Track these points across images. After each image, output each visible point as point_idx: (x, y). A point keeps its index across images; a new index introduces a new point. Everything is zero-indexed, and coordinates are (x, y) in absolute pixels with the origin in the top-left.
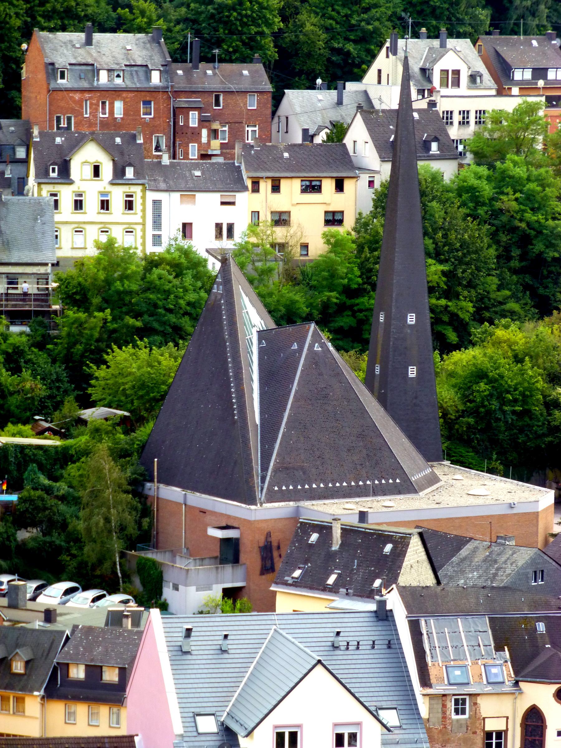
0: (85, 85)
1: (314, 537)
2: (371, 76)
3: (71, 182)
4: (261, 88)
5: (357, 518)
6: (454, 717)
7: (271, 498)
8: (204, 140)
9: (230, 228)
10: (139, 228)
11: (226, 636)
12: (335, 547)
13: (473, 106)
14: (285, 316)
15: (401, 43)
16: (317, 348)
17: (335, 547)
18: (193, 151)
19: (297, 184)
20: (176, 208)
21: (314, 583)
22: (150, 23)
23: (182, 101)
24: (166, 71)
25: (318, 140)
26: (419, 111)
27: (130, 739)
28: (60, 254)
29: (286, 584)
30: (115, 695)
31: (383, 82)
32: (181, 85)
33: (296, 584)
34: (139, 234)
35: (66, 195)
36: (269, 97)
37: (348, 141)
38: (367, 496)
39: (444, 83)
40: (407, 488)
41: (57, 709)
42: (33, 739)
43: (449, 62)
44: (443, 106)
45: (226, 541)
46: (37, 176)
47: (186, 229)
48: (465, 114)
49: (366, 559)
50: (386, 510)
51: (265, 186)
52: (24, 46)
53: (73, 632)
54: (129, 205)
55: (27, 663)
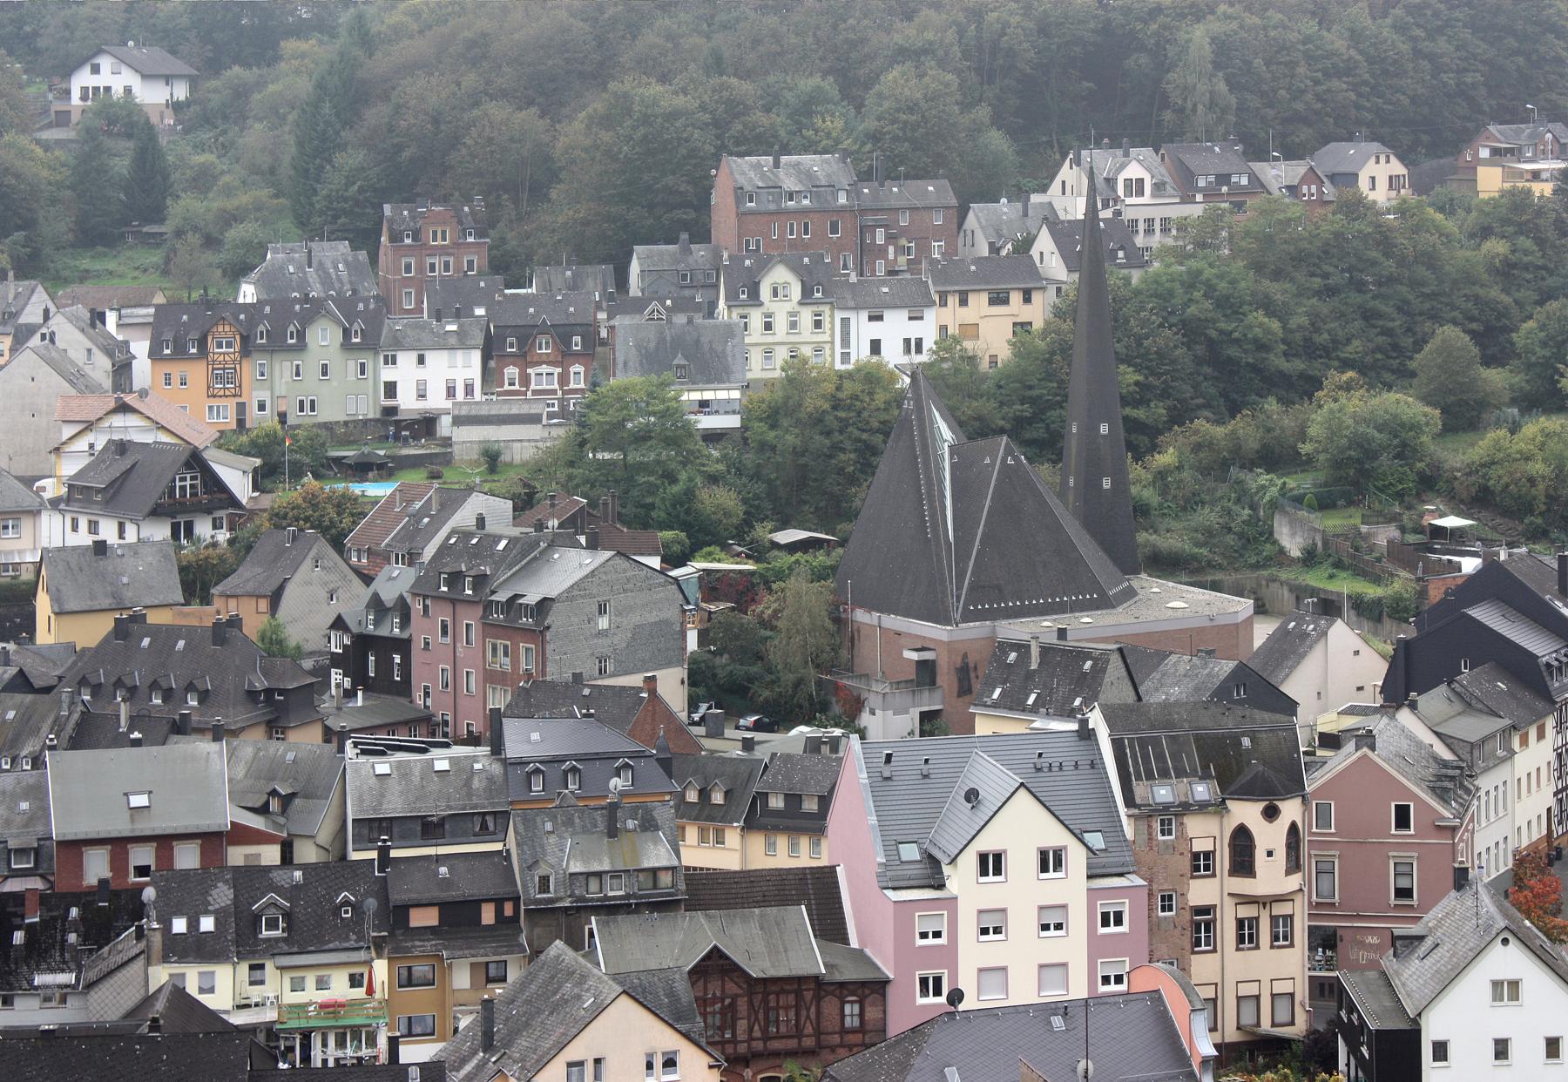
0: (772, 207)
1: (1013, 656)
2: (1056, 187)
3: (761, 304)
4: (944, 202)
5: (1055, 635)
6: (1160, 838)
7: (967, 617)
8: (891, 256)
9: (919, 342)
10: (827, 347)
11: (927, 761)
12: (1034, 666)
13: (1157, 214)
14: (974, 430)
15: (1084, 153)
16: (1010, 461)
17: (1034, 666)
18: (880, 267)
19: (985, 297)
20: (864, 330)
21: (1012, 702)
22: (837, 142)
23: (870, 219)
24: (854, 192)
25: (1004, 253)
26: (1104, 220)
27: (831, 871)
28: (749, 376)
29: (985, 705)
30: (815, 825)
31: (1068, 195)
32: (868, 204)
33: (995, 705)
34: (828, 352)
35: (756, 319)
36: (954, 212)
37: (1035, 252)
38: (1064, 612)
39: (1129, 193)
40: (1104, 603)
41: (757, 841)
42: (735, 872)
43: (1134, 171)
44: (1128, 214)
45: (921, 664)
46: (727, 299)
47: (876, 346)
48: (1150, 222)
49: (1064, 677)
50: (1088, 627)
51: (953, 301)
52: (713, 172)
53: (771, 759)
54: (818, 324)
55: (726, 793)
